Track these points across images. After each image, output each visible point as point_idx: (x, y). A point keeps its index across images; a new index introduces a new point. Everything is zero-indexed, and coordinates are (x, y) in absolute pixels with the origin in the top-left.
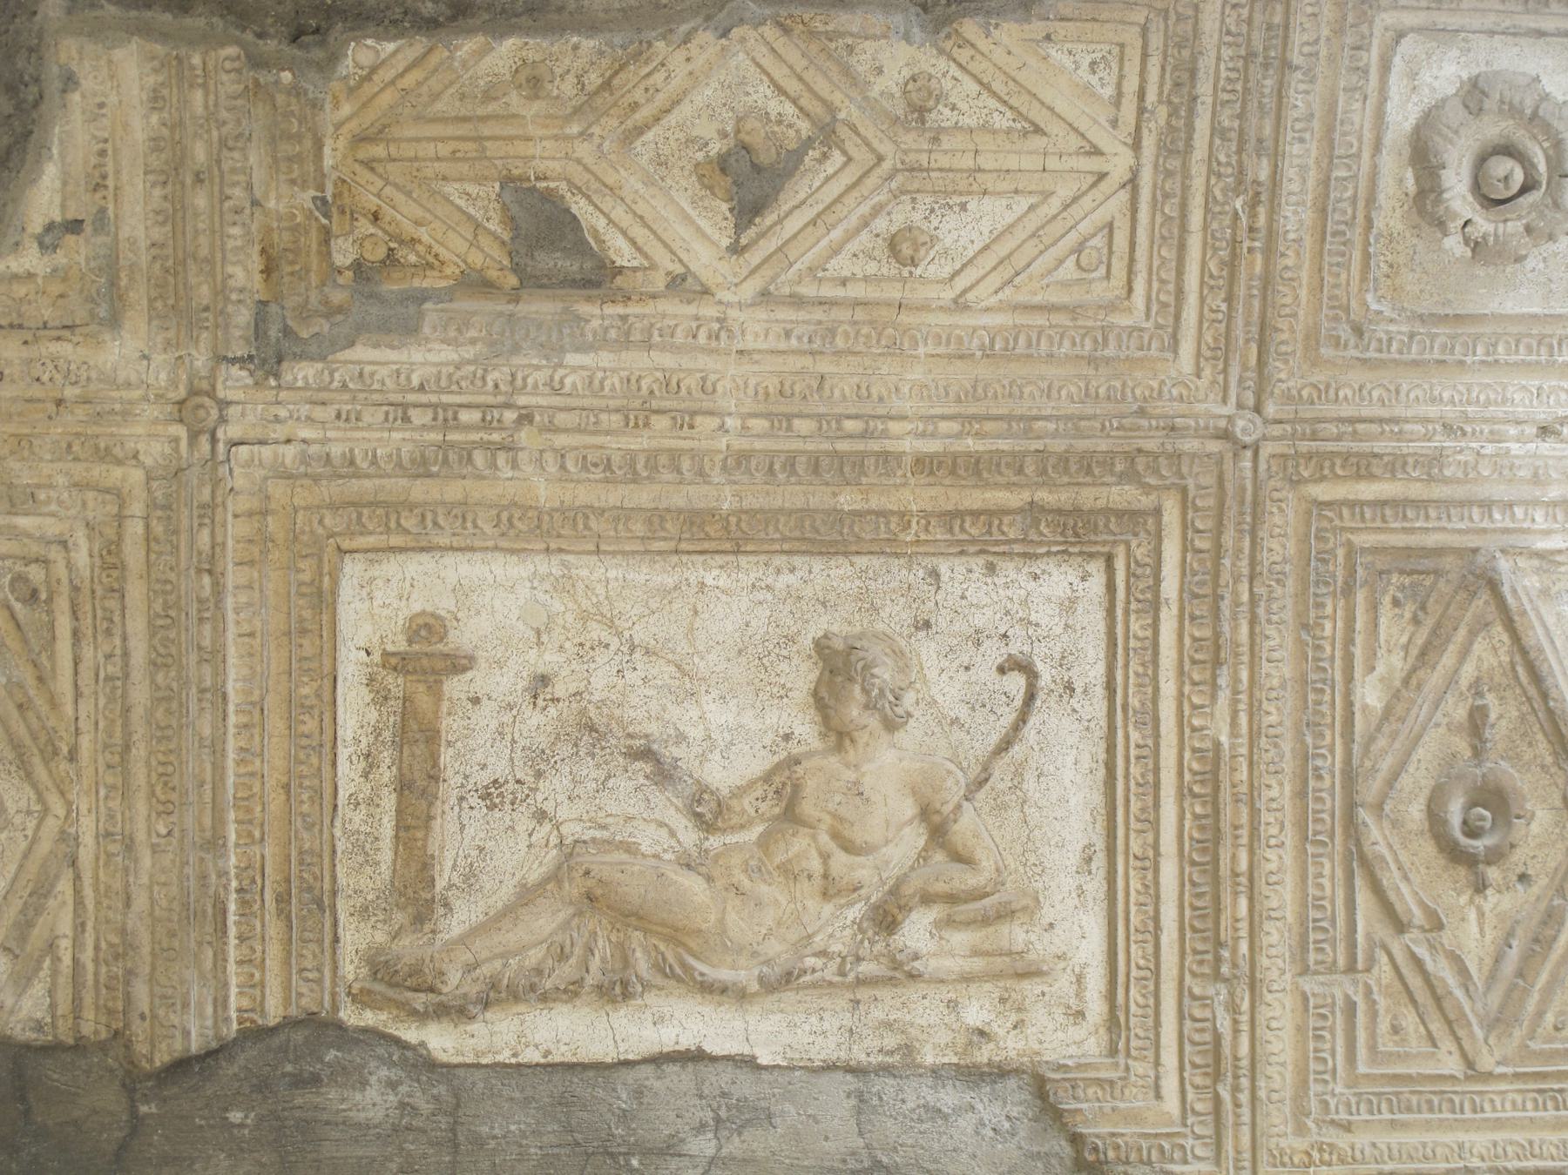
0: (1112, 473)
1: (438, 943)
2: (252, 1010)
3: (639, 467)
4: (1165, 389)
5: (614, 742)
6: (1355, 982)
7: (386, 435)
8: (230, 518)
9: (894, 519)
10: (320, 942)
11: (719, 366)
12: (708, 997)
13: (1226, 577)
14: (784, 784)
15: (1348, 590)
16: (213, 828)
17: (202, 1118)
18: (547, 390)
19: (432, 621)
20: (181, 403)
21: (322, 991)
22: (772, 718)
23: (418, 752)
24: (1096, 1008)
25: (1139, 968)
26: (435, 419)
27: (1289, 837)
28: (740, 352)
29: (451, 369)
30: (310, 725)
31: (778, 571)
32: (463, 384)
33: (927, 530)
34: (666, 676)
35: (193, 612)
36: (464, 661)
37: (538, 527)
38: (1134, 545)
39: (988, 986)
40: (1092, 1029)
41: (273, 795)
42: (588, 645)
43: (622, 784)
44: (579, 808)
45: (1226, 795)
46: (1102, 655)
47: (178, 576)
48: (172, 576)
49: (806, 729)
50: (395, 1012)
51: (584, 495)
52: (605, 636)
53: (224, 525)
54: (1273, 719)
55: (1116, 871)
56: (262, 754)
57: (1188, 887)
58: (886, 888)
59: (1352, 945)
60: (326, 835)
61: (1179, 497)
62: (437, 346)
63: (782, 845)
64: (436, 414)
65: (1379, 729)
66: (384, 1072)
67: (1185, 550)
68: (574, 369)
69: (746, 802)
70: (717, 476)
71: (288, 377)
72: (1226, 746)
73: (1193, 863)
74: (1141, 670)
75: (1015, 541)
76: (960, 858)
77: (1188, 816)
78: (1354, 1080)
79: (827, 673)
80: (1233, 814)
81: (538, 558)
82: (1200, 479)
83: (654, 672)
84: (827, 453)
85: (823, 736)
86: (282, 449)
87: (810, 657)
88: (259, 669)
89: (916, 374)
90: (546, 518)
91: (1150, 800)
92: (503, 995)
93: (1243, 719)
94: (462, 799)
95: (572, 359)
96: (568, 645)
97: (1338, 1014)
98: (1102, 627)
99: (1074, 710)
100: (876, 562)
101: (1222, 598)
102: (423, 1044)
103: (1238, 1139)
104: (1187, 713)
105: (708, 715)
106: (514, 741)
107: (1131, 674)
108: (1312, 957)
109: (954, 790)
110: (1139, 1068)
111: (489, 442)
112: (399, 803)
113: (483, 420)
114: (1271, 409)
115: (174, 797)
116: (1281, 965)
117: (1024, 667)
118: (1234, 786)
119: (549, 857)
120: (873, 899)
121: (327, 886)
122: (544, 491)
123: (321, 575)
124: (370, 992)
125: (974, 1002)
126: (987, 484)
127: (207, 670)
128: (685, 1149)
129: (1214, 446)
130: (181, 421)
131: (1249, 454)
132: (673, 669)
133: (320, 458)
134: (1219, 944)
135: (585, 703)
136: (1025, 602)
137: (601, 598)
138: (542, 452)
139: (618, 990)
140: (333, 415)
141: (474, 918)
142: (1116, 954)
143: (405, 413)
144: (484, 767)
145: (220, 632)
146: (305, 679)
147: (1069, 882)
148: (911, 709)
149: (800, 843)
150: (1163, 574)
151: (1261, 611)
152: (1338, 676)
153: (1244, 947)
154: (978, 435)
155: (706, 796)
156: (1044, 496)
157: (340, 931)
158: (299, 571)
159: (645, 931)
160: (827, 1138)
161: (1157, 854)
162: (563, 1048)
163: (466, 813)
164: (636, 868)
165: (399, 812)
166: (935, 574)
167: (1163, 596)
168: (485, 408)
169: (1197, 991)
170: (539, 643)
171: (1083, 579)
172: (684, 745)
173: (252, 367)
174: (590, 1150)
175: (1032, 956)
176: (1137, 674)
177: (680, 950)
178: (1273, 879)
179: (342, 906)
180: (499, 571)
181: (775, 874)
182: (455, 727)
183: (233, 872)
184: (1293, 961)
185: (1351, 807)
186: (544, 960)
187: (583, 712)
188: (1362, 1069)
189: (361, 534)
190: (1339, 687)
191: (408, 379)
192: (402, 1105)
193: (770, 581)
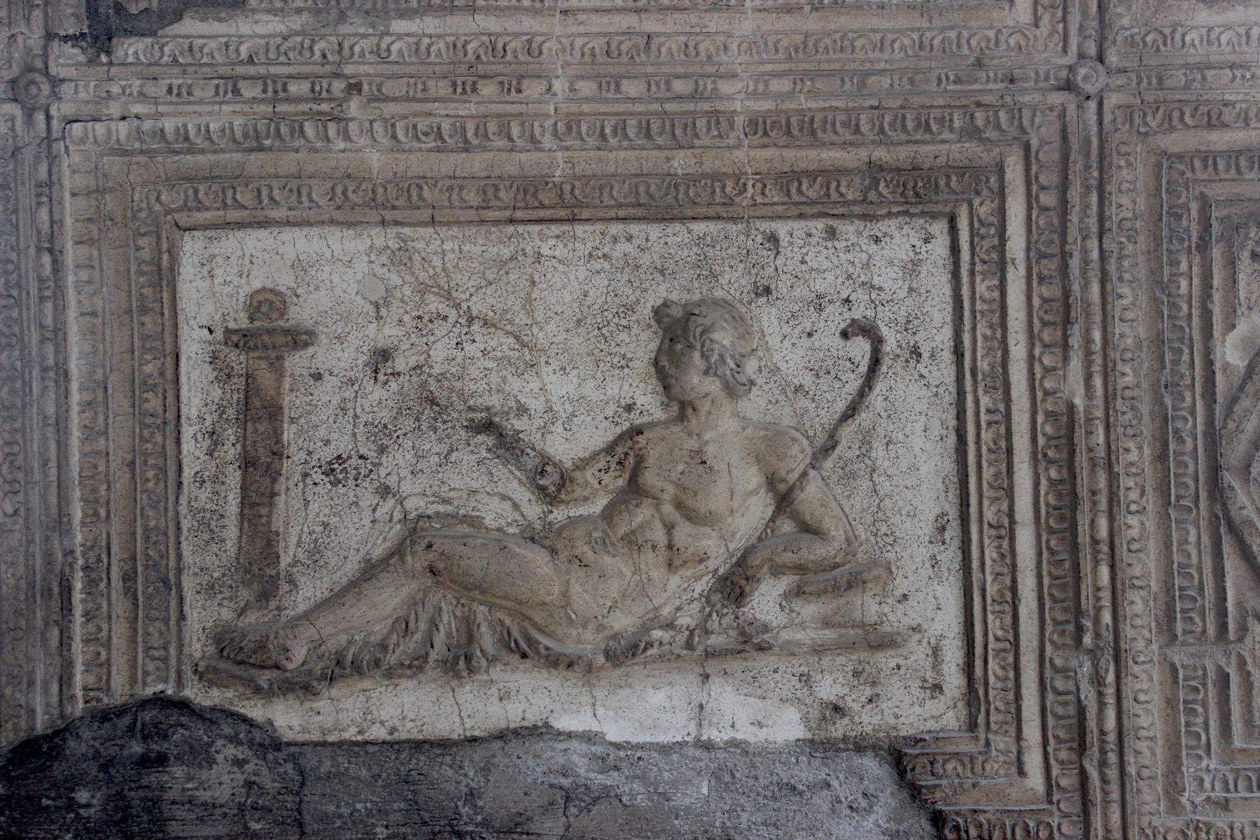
0: (951, 129)
1: (283, 619)
2: (99, 689)
3: (470, 134)
4: (1003, 39)
5: (455, 415)
6: (1227, 654)
7: (216, 108)
8: (67, 195)
9: (730, 184)
10: (166, 621)
11: (544, 29)
12: (554, 672)
13: (1073, 233)
14: (626, 454)
15: (1203, 246)
16: (59, 506)
17: (48, 798)
18: (373, 58)
19: (271, 297)
20: (13, 82)
21: (168, 669)
22: (613, 389)
23: (261, 429)
24: (954, 681)
25: (997, 639)
26: (265, 91)
27: (1151, 502)
28: (565, 12)
29: (279, 40)
30: (154, 403)
31: (615, 240)
32: (291, 55)
33: (763, 194)
34: (505, 348)
35: (34, 291)
36: (304, 337)
37: (373, 200)
38: (976, 202)
39: (841, 660)
40: (951, 703)
41: (119, 473)
42: (426, 318)
43: (465, 457)
44: (423, 482)
45: (1082, 460)
46: (949, 319)
47: (18, 255)
48: (14, 256)
49: (649, 402)
50: (241, 690)
51: (415, 164)
52: (443, 308)
53: (61, 202)
54: (1129, 379)
55: (970, 540)
56: (106, 433)
57: (1045, 555)
58: (734, 560)
59: (1222, 614)
60: (171, 514)
61: (1022, 153)
62: (264, 17)
63: (626, 516)
64: (265, 85)
65: (1242, 388)
66: (231, 751)
67: (1029, 209)
68: (400, 37)
69: (589, 474)
70: (548, 142)
71: (119, 53)
72: (1081, 409)
73: (1051, 531)
74: (989, 332)
75: (855, 202)
76: (809, 529)
77: (1044, 482)
78: (1229, 755)
79: (667, 342)
80: (1091, 480)
81: (374, 231)
82: (1044, 133)
83: (493, 343)
84: (656, 113)
85: (665, 406)
86: (113, 125)
87: (650, 326)
88: (101, 347)
89: (746, 26)
90: (380, 191)
91: (1003, 468)
92: (348, 671)
93: (1098, 382)
94: (306, 475)
95: (398, 26)
96: (406, 318)
97: (1210, 687)
98: (947, 290)
99: (921, 376)
100: (713, 227)
101: (1071, 255)
102: (270, 723)
103: (1106, 818)
104: (1038, 376)
105: (549, 387)
106: (356, 416)
107: (979, 338)
108: (1179, 627)
109: (797, 458)
110: (1001, 742)
111: (319, 113)
112: (244, 479)
113: (313, 90)
114: (1113, 58)
115: (20, 476)
116: (1147, 635)
117: (867, 330)
118: (1090, 450)
119: (394, 531)
120: (721, 572)
121: (172, 564)
122: (376, 160)
123: (160, 252)
124: (215, 670)
125: (827, 676)
126: (824, 144)
127: (50, 348)
128: (533, 827)
129: (1056, 98)
130: (15, 100)
131: (1092, 105)
132: (512, 340)
133: (155, 133)
134: (1078, 612)
135: (424, 377)
136: (866, 266)
137: (438, 270)
138: (371, 122)
139: (462, 664)
140: (164, 90)
141: (318, 594)
142: (972, 625)
143: (235, 85)
144: (327, 443)
145: (60, 310)
146: (148, 357)
147: (922, 553)
148: (754, 377)
149: (644, 513)
150: (1008, 233)
151: (1112, 268)
152: (1196, 336)
153: (1107, 617)
154: (813, 94)
155: (548, 468)
156: (881, 154)
157: (186, 608)
158: (138, 249)
159: (491, 606)
160: (677, 817)
161: (1012, 522)
162: (409, 725)
163: (310, 490)
164: (479, 541)
165: (244, 488)
166: (773, 239)
167: (1009, 255)
168: (313, 78)
169: (1059, 662)
170: (379, 318)
171: (926, 241)
172: (525, 418)
173: (84, 44)
174: (437, 829)
175: (886, 628)
176: (985, 337)
177: (526, 624)
178: (1135, 546)
179: (188, 584)
180: (336, 246)
181: (619, 545)
182: (298, 402)
183: (79, 550)
184: (1160, 632)
185: (1215, 470)
186: (388, 636)
187: (424, 385)
188: (1238, 743)
189: (199, 210)
190: (1198, 346)
191: (237, 51)
192: (249, 784)
193: (606, 250)
